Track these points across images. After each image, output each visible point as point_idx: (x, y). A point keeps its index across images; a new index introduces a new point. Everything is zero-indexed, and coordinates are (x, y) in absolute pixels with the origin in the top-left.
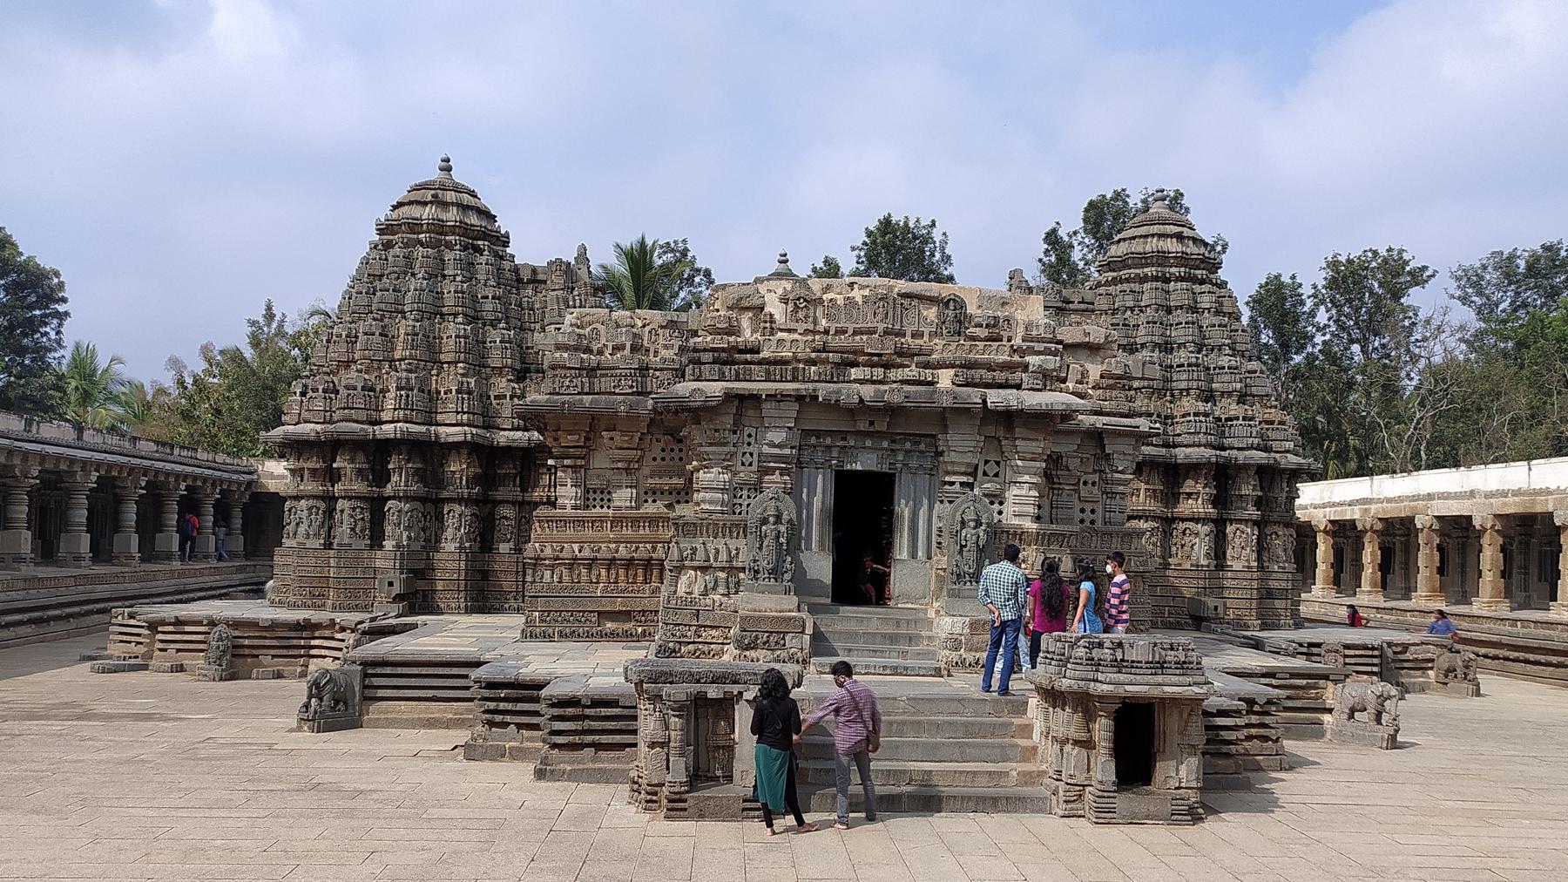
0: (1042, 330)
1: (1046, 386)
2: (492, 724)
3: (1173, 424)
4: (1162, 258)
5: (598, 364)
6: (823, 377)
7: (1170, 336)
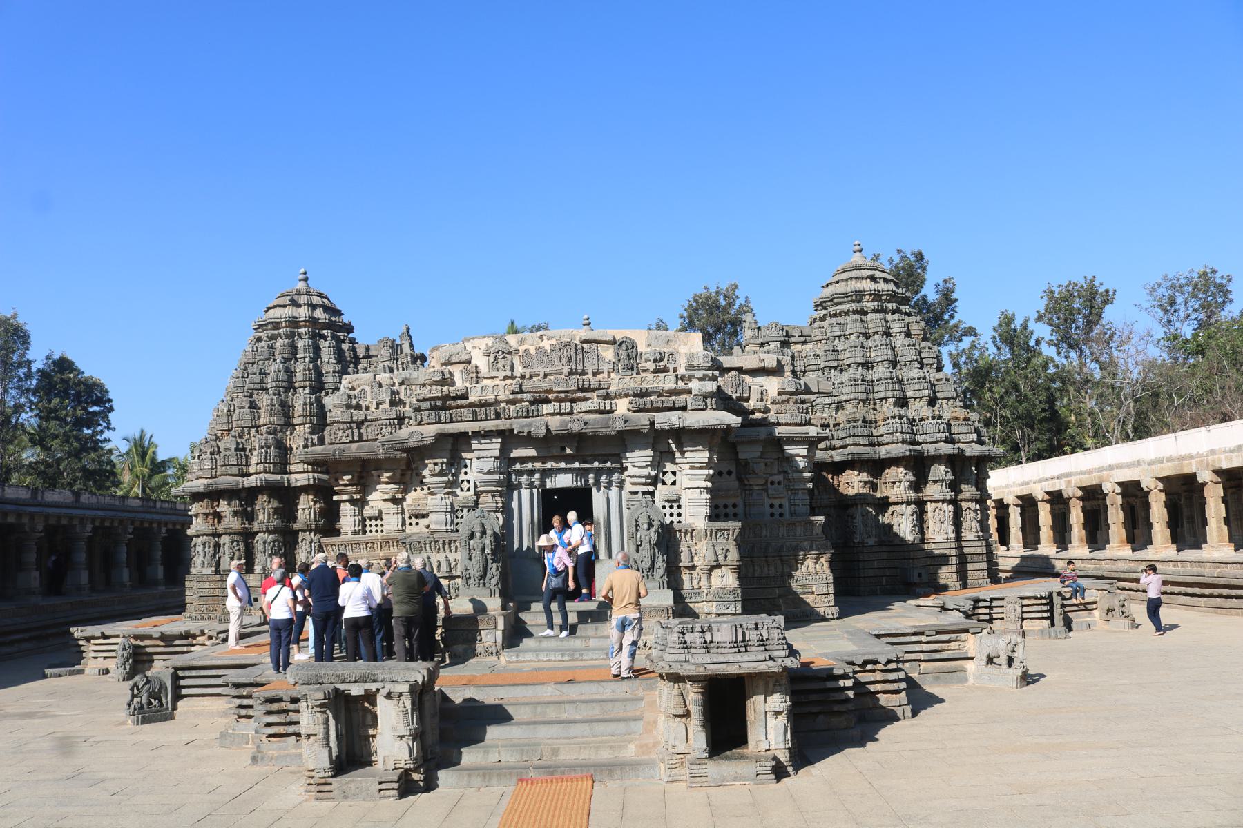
0: (701, 360)
1: (707, 407)
2: (240, 717)
3: (876, 427)
4: (859, 296)
5: (366, 417)
6: (520, 414)
7: (870, 357)
